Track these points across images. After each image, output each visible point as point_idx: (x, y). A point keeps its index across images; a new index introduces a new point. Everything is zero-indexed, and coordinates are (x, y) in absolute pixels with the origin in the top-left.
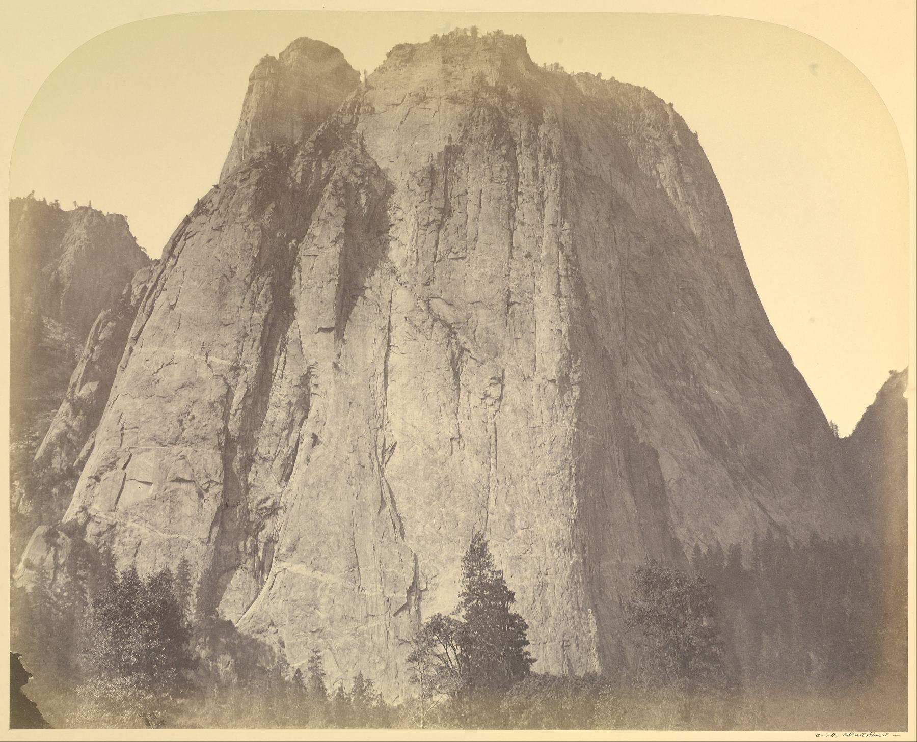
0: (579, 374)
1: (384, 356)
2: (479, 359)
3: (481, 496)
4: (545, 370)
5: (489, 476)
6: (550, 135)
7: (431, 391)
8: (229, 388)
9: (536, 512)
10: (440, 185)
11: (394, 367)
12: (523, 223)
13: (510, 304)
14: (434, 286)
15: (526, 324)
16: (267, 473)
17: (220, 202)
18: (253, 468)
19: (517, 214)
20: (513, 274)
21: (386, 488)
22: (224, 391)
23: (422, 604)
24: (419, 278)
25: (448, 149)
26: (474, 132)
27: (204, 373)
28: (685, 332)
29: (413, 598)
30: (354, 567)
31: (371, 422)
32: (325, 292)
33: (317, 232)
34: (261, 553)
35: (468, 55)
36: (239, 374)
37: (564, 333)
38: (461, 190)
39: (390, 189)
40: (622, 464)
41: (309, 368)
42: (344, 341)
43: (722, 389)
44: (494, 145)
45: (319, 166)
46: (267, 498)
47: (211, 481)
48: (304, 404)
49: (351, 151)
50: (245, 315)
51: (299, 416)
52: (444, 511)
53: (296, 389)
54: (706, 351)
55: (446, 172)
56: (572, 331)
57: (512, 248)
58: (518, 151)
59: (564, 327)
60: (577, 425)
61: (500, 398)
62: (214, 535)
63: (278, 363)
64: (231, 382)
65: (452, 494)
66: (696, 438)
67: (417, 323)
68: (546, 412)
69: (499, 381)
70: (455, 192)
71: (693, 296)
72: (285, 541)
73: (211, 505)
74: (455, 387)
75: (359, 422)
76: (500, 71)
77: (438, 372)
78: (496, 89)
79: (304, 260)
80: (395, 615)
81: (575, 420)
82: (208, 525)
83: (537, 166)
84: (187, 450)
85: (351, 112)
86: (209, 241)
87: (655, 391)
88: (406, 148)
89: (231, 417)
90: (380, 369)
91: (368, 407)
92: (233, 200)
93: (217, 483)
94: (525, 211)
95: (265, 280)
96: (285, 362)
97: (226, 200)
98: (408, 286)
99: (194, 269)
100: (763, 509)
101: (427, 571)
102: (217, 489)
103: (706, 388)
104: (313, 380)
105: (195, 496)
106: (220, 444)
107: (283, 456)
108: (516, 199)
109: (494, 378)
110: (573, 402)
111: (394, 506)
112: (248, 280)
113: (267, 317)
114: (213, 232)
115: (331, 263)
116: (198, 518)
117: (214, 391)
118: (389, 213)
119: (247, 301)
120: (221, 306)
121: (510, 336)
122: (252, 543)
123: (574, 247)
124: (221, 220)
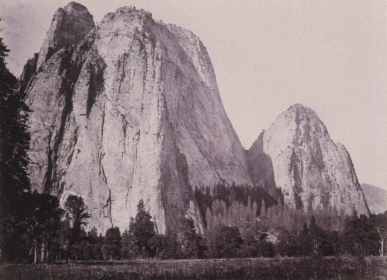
0: (163, 133)
1: (102, 124)
2: (132, 126)
3: (131, 171)
4: (153, 131)
5: (134, 165)
6: (158, 52)
7: (117, 137)
8: (51, 133)
9: (148, 177)
10: (122, 66)
11: (105, 128)
12: (148, 81)
13: (142, 108)
14: (119, 101)
15: (148, 115)
16: (63, 161)
17: (48, 68)
18: (58, 160)
19: (147, 78)
20: (144, 98)
21: (101, 168)
22: (49, 134)
23: (112, 205)
24: (114, 98)
25: (125, 54)
26: (133, 48)
27: (42, 128)
28: (197, 115)
29: (109, 203)
30: (90, 193)
31: (97, 146)
32: (83, 102)
33: (81, 81)
34: (60, 188)
35: (133, 19)
36: (54, 129)
37: (159, 119)
38: (129, 69)
39: (105, 66)
40: (175, 161)
41: (77, 128)
42: (89, 119)
43: (208, 134)
44: (140, 53)
45: (81, 56)
46: (63, 170)
47: (44, 164)
48: (75, 139)
49: (92, 52)
50: (56, 108)
51: (73, 143)
52: (119, 176)
53: (72, 134)
54: (204, 122)
55: (124, 62)
56: (162, 119)
57: (144, 89)
58: (148, 56)
59: (160, 117)
60: (162, 149)
61: (138, 139)
62: (45, 181)
63: (67, 125)
64: (51, 131)
65: (122, 170)
66: (199, 151)
67: (113, 114)
68: (152, 144)
69: (139, 134)
70: (127, 70)
71: (201, 104)
72: (68, 184)
73: (44, 172)
74: (124, 135)
75: (93, 146)
76: (143, 26)
77: (119, 130)
78: (141, 33)
79: (76, 91)
80: (103, 208)
81: (161, 147)
82: (43, 178)
83: (153, 62)
84: (36, 153)
85: (92, 37)
86: (44, 82)
87: (187, 135)
88: (110, 52)
89: (51, 143)
90: (101, 129)
91: (97, 141)
92: (53, 68)
93: (46, 165)
94: (149, 76)
95: (63, 97)
96: (69, 125)
97: (50, 68)
98: (110, 101)
99: (38, 92)
100: (219, 175)
101: (113, 195)
102: (46, 167)
103: (203, 134)
104: (78, 131)
105: (39, 169)
106: (47, 152)
107: (68, 156)
108: (146, 72)
109: (137, 133)
110: (161, 142)
111: (104, 174)
112: (57, 96)
113: (64, 109)
114: (46, 79)
115: (86, 92)
116: (40, 176)
117: (45, 134)
118: (104, 75)
119: (57, 103)
120: (48, 105)
121: (142, 119)
122: (57, 184)
123: (164, 90)
124: (48, 74)
